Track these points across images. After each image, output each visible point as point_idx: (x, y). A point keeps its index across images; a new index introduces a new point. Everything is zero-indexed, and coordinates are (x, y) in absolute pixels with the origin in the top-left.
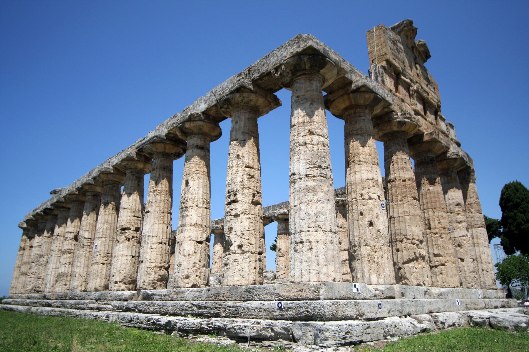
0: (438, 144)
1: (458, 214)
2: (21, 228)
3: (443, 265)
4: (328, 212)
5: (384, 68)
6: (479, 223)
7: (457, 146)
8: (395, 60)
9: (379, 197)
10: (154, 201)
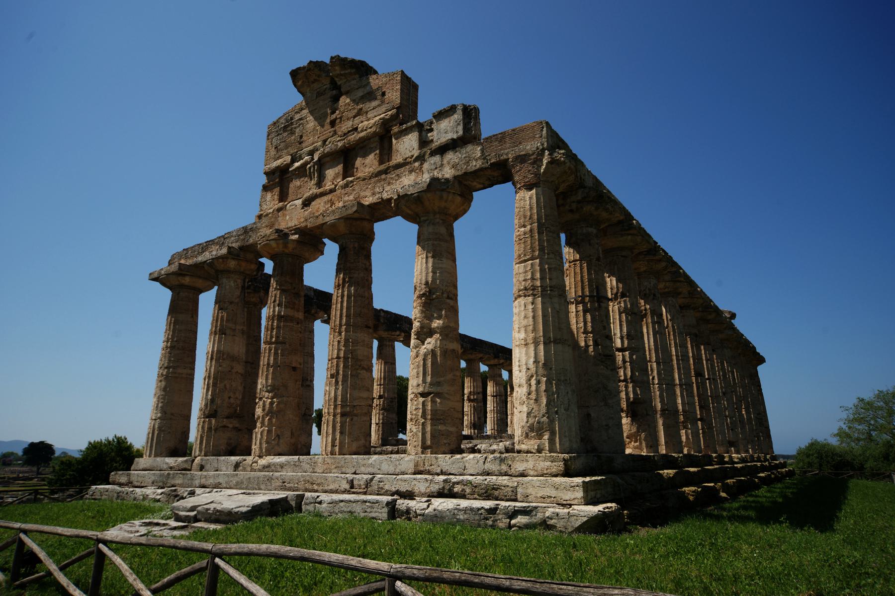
0: (324, 226)
7: (437, 158)
8: (279, 158)
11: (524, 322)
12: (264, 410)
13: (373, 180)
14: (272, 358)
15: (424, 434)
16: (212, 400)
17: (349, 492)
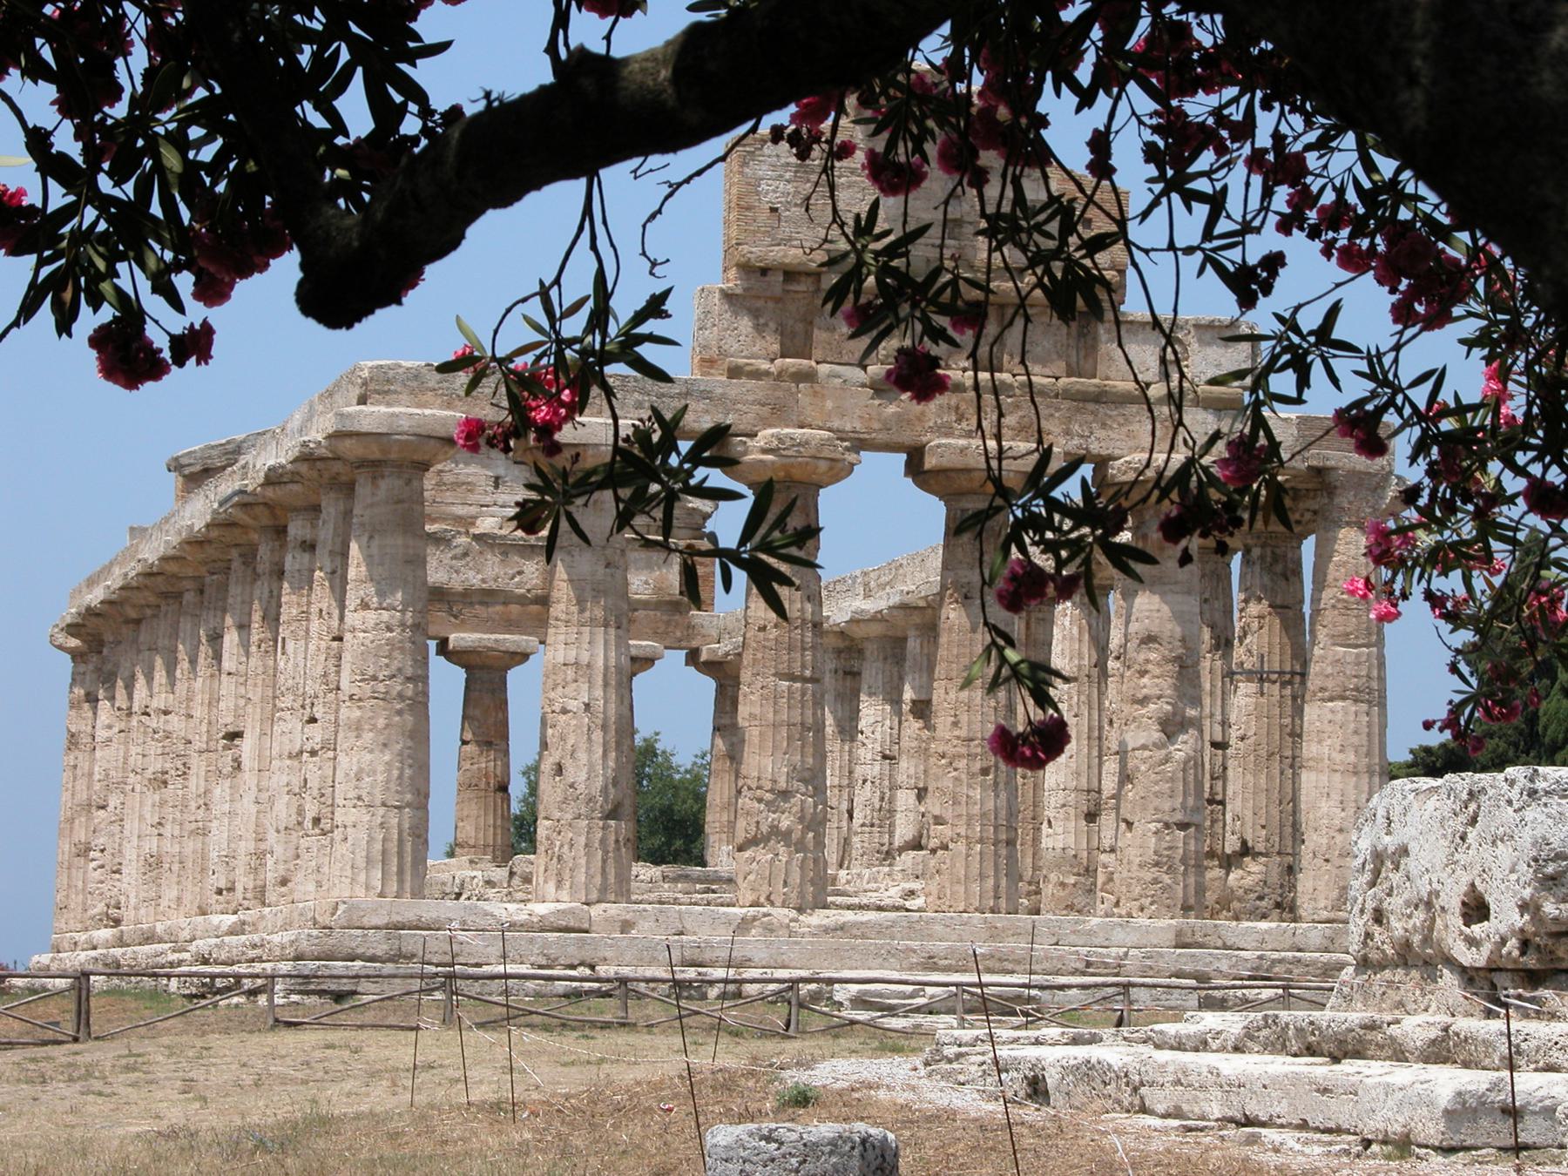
1: (1143, 673)
2: (60, 647)
3: (946, 848)
4: (381, 768)
5: (728, 296)
6: (1330, 684)
9: (587, 706)
10: (260, 670)
11: (1355, 740)
12: (801, 819)
13: (1066, 404)
14: (809, 713)
15: (1185, 887)
16: (615, 783)
17: (1084, 974)
